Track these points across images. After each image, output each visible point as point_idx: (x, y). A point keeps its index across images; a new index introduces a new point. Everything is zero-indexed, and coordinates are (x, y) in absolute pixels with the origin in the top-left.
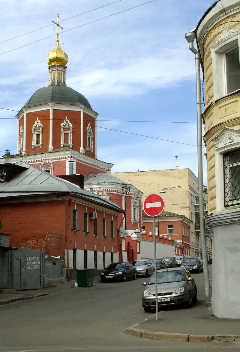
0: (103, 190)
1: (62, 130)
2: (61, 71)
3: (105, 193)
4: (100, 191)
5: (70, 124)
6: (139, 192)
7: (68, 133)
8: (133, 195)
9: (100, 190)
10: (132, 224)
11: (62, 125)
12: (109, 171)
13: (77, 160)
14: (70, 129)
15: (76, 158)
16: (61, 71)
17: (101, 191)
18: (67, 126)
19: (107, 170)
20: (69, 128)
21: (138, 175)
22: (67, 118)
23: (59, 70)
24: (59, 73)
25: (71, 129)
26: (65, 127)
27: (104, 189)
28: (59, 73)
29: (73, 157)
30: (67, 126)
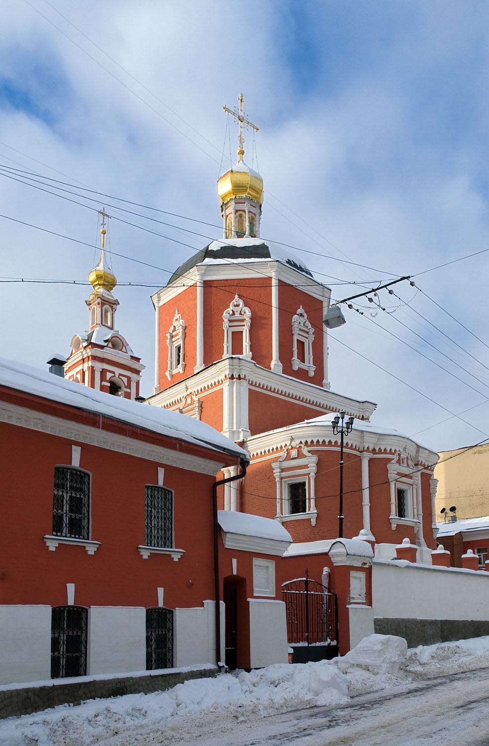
0: (301, 443)
1: (226, 324)
3: (305, 450)
4: (292, 448)
6: (417, 452)
7: (242, 332)
8: (393, 454)
9: (294, 444)
10: (394, 527)
13: (252, 384)
15: (245, 378)
16: (244, 211)
17: (295, 448)
21: (480, 452)
23: (240, 210)
24: (241, 216)
26: (233, 318)
27: (303, 442)
29: (237, 376)
30: (237, 315)
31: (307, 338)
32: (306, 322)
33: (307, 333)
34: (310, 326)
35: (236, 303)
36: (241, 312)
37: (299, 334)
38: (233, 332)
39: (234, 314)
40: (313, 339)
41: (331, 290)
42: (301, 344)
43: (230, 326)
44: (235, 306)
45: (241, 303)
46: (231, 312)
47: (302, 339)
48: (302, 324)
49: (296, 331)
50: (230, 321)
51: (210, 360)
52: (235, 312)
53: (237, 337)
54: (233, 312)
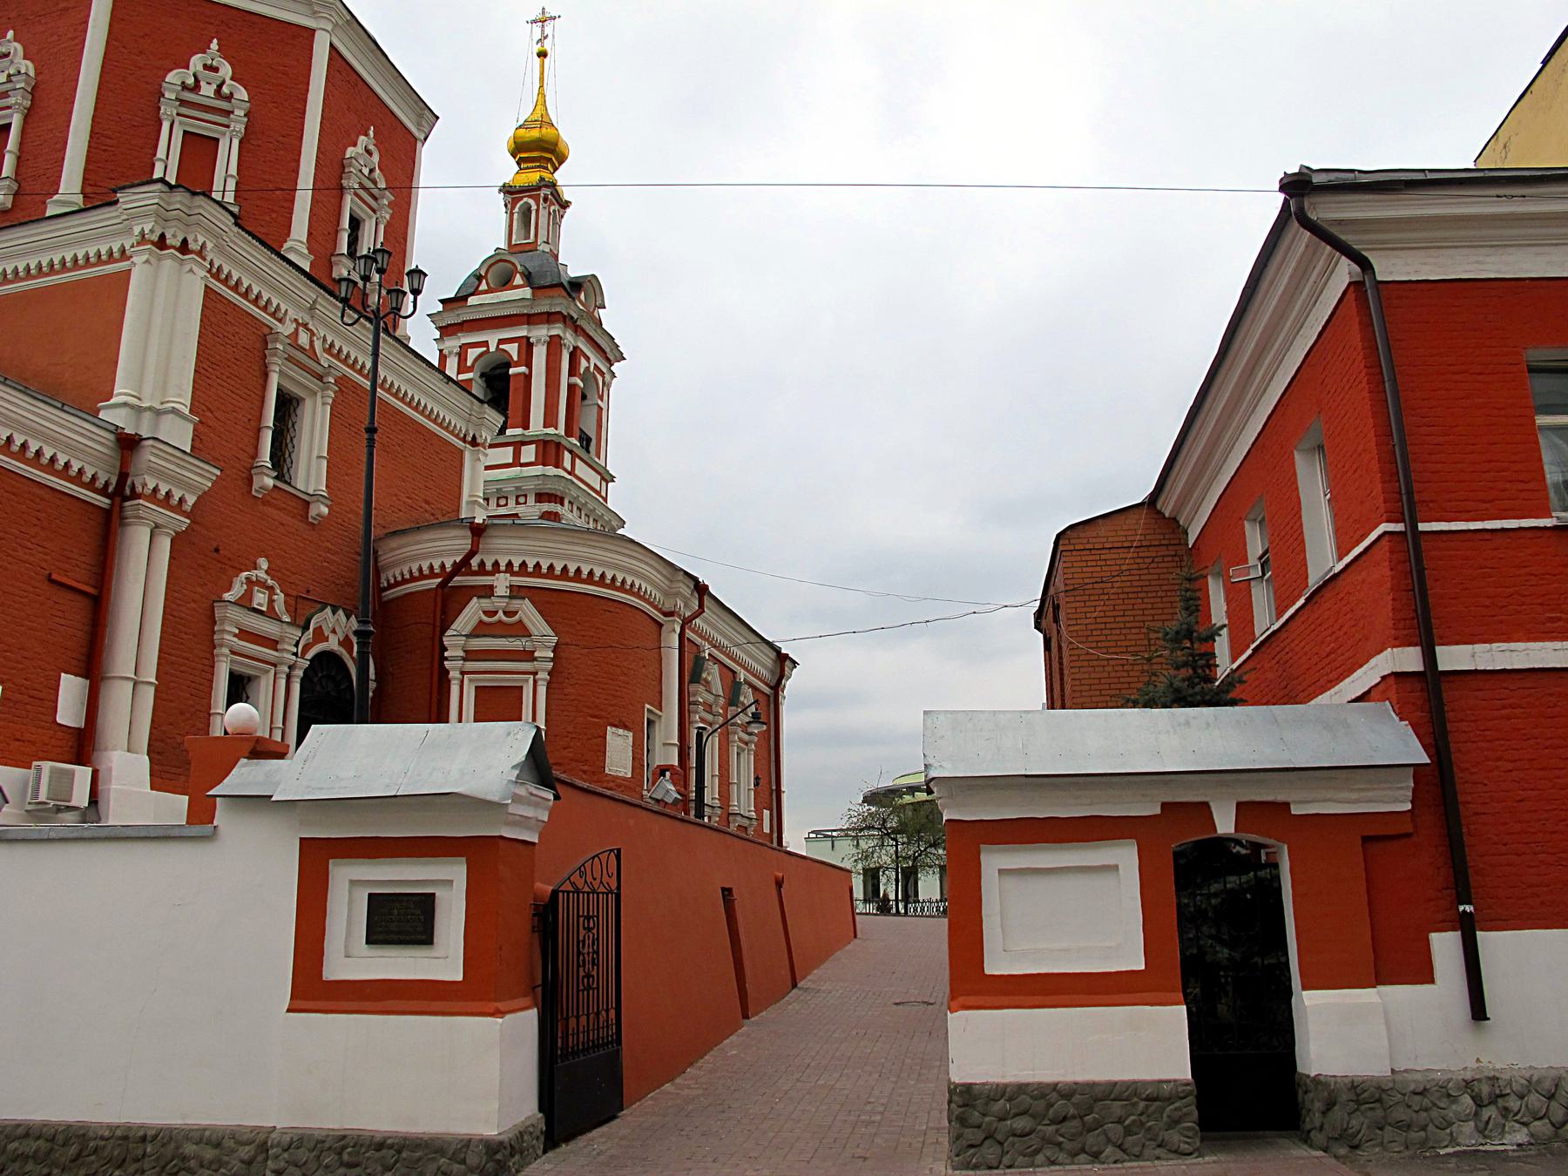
7: (217, 140)
12: (478, 445)
14: (233, 112)
18: (208, 90)
19: (464, 439)
22: (214, 45)
30: (208, 90)
31: (374, 211)
33: (376, 199)
35: (209, 62)
36: (220, 86)
37: (356, 195)
39: (196, 88)
40: (388, 217)
41: (437, 118)
43: (178, 114)
44: (205, 67)
45: (226, 70)
46: (191, 81)
51: (99, 194)
52: (203, 84)
53: (199, 150)
54: (197, 81)
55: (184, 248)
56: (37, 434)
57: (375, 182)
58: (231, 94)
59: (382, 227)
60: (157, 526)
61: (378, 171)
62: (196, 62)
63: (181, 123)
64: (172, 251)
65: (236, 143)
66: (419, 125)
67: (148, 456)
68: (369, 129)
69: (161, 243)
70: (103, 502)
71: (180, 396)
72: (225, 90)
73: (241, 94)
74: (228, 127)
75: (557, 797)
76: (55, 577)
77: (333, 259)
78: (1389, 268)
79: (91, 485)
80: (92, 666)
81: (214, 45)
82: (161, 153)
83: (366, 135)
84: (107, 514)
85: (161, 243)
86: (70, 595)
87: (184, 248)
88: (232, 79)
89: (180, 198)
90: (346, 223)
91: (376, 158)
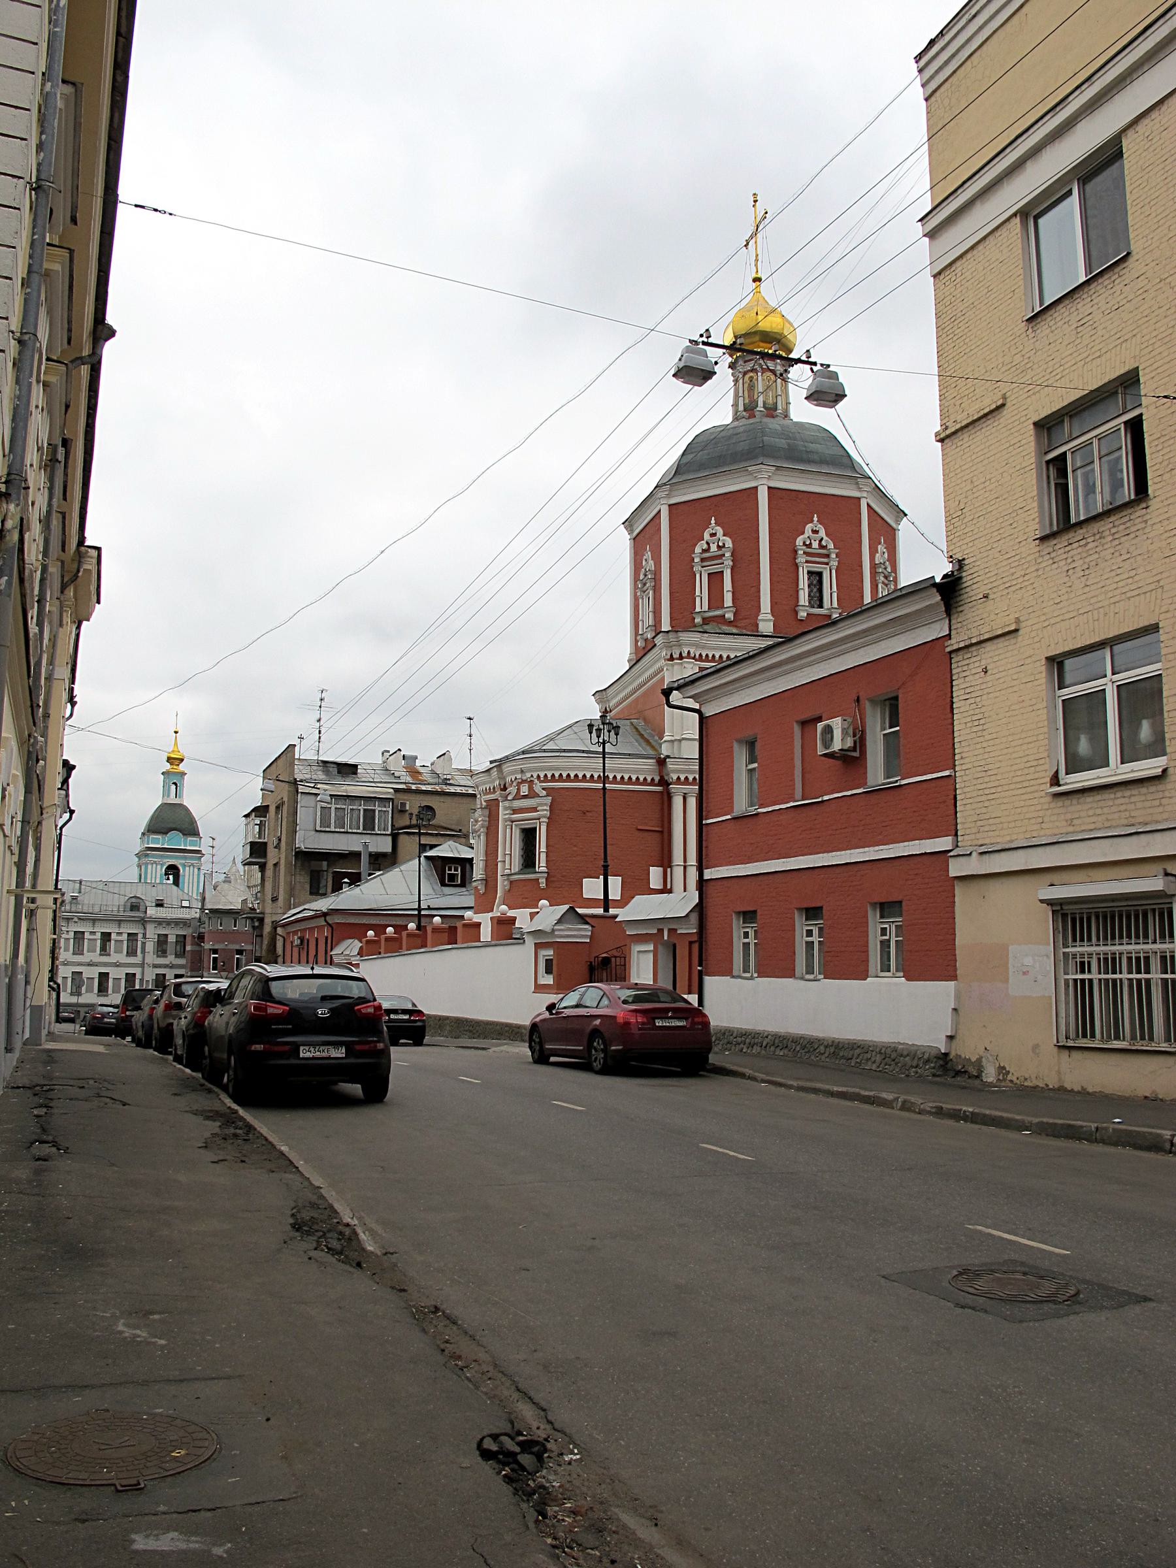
2: (753, 370)
5: (723, 540)
11: (698, 550)
14: (724, 555)
18: (714, 548)
20: (720, 553)
22: (713, 521)
25: (728, 555)
28: (751, 379)
30: (714, 548)
31: (827, 564)
32: (822, 539)
33: (828, 556)
34: (831, 546)
37: (807, 562)
38: (709, 574)
39: (707, 550)
40: (836, 564)
42: (816, 578)
45: (720, 531)
46: (705, 546)
47: (816, 568)
48: (815, 545)
49: (801, 559)
50: (703, 560)
53: (716, 578)
54: (708, 543)
55: (681, 657)
56: (620, 771)
57: (825, 547)
58: (724, 544)
59: (834, 572)
60: (685, 794)
61: (825, 538)
62: (706, 536)
63: (705, 570)
64: (676, 661)
65: (729, 571)
66: (859, 489)
67: (671, 765)
68: (813, 517)
69: (672, 658)
70: (659, 789)
71: (688, 730)
72: (720, 544)
73: (729, 543)
74: (723, 563)
75: (592, 926)
76: (640, 827)
77: (797, 608)
78: (709, 711)
79: (652, 783)
80: (666, 862)
81: (713, 521)
82: (698, 593)
83: (812, 521)
84: (661, 793)
85: (672, 658)
86: (651, 833)
87: (681, 657)
88: (724, 535)
89: (671, 635)
90: (803, 581)
91: (822, 533)
